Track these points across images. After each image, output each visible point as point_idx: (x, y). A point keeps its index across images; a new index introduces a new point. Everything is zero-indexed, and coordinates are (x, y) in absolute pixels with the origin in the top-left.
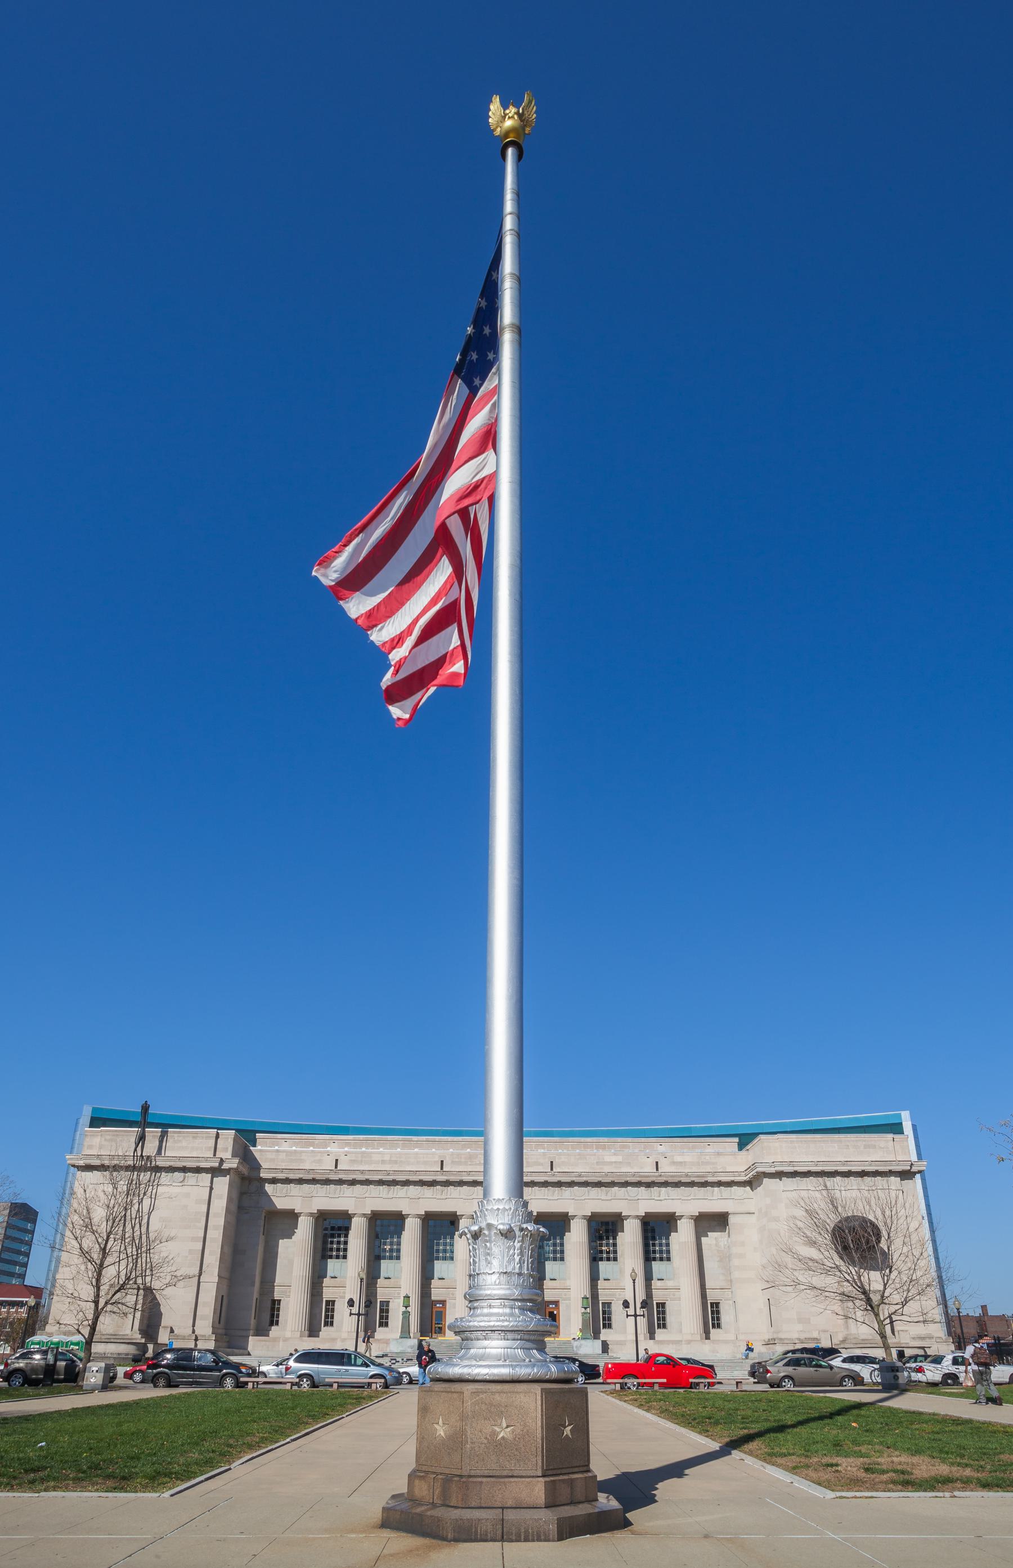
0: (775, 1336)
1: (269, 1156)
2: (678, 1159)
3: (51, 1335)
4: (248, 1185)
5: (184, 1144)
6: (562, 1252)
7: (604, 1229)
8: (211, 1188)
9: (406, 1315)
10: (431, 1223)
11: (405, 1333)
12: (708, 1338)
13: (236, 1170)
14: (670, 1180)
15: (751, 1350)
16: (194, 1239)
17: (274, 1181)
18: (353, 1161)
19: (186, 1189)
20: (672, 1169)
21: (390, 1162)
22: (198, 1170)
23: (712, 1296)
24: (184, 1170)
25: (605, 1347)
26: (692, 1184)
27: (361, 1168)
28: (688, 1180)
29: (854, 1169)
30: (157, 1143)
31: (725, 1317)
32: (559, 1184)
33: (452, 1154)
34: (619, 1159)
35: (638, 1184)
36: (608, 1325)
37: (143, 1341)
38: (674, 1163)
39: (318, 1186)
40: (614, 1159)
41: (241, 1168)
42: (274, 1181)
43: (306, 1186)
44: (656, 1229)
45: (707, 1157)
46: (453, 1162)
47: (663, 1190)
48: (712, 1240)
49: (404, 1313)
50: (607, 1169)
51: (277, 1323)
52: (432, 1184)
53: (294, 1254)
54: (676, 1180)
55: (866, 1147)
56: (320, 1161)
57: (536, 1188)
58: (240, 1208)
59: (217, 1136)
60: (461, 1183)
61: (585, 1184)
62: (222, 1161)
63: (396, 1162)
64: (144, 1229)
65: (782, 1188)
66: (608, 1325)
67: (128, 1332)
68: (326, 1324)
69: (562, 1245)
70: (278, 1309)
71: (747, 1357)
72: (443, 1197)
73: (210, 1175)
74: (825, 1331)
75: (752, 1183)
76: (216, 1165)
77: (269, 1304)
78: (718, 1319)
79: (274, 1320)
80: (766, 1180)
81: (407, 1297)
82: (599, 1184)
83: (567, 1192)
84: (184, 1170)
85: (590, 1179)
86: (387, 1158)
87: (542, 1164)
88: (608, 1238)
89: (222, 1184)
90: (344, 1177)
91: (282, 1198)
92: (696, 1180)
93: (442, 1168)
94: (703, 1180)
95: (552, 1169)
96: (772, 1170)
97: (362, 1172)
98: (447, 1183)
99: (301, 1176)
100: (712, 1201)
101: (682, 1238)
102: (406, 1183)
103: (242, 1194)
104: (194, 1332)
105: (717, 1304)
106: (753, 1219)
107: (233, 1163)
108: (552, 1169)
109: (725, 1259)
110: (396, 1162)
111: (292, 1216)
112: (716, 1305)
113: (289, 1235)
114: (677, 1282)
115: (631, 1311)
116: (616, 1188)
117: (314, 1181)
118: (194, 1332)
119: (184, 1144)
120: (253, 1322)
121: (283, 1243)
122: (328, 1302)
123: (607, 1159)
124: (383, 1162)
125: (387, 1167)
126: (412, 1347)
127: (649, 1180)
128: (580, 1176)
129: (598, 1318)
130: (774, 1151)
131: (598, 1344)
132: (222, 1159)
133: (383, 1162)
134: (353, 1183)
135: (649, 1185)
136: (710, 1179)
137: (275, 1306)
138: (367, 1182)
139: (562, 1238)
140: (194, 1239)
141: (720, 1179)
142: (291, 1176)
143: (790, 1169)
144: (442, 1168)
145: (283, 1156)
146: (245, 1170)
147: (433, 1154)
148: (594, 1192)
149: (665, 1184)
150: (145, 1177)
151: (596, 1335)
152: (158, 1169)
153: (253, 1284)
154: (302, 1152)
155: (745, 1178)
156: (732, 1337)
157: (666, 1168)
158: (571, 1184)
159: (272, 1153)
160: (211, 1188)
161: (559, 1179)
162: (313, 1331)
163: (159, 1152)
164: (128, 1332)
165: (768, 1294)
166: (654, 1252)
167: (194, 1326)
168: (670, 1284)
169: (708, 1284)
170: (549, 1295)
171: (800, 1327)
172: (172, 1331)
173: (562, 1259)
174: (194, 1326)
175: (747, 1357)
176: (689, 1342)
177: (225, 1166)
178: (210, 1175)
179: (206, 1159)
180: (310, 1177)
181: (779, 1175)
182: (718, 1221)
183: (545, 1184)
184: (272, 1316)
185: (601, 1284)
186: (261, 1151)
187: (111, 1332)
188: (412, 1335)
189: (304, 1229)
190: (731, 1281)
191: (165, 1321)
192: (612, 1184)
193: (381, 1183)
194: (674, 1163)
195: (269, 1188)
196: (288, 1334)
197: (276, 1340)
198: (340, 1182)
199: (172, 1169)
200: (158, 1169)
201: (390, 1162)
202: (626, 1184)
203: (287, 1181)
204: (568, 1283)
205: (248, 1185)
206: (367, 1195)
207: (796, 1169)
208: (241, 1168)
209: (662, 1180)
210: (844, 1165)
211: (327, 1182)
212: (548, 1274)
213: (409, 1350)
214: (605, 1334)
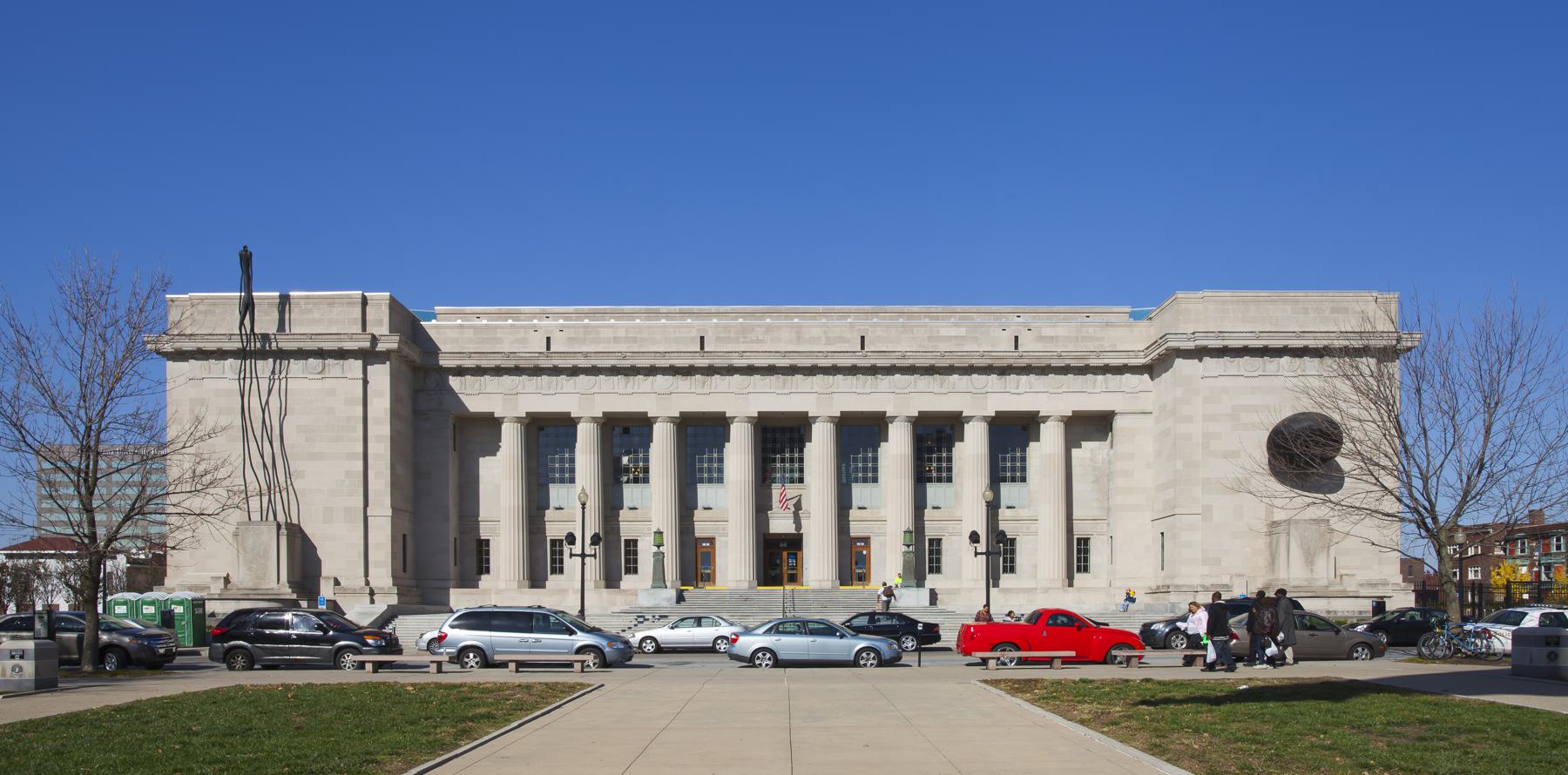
0: (1168, 582)
1: (450, 334)
2: (1048, 331)
3: (171, 591)
4: (421, 376)
5: (316, 315)
6: (875, 470)
7: (935, 438)
8: (365, 382)
9: (659, 558)
10: (690, 430)
11: (659, 580)
12: (1071, 585)
13: (398, 351)
14: (1035, 363)
15: (1132, 600)
16: (350, 456)
17: (460, 371)
18: (571, 340)
19: (328, 383)
20: (1039, 347)
21: (628, 340)
22: (342, 354)
23: (1079, 530)
24: (321, 354)
25: (933, 597)
26: (1065, 370)
27: (584, 349)
28: (1061, 363)
29: (1311, 343)
30: (276, 315)
31: (1096, 557)
32: (873, 370)
33: (717, 326)
34: (962, 332)
35: (988, 370)
36: (936, 569)
37: (294, 596)
38: (1041, 338)
39: (525, 377)
40: (953, 332)
41: (406, 350)
42: (460, 371)
43: (507, 379)
44: (1012, 433)
45: (1091, 330)
46: (718, 339)
47: (1024, 378)
48: (1088, 452)
49: (656, 554)
50: (943, 347)
51: (488, 571)
52: (689, 371)
53: (500, 477)
54: (1043, 363)
55: (1333, 311)
56: (524, 341)
57: (840, 377)
58: (417, 412)
59: (365, 302)
60: (730, 370)
61: (911, 370)
62: (374, 340)
63: (634, 340)
64: (277, 444)
65: (1201, 373)
66: (936, 569)
67: (273, 584)
68: (554, 571)
69: (875, 460)
70: (488, 553)
71: (1126, 610)
72: (706, 391)
73: (359, 363)
74: (1240, 575)
75: (1153, 369)
76: (368, 344)
77: (474, 546)
78: (1086, 560)
79: (483, 567)
80: (1179, 362)
81: (659, 533)
82: (930, 370)
83: (885, 382)
84: (321, 354)
85: (920, 362)
86: (621, 333)
87: (848, 341)
88: (940, 450)
89: (381, 375)
90: (562, 363)
91: (477, 396)
92: (1074, 363)
93: (702, 347)
94: (1081, 363)
95: (863, 347)
96: (1191, 345)
97: (586, 355)
98: (710, 371)
99: (498, 363)
100: (1091, 395)
101: (1045, 449)
102: (651, 371)
103: (416, 392)
104: (367, 583)
105: (1086, 541)
106: (1148, 422)
107: (389, 343)
108: (863, 347)
109: (1104, 478)
110: (634, 340)
111: (491, 423)
112: (1084, 542)
113: (493, 449)
114: (1034, 511)
115: (982, 547)
116: (956, 376)
117: (517, 371)
118: (367, 583)
119: (316, 315)
120: (453, 570)
121: (486, 464)
122: (553, 542)
123: (944, 332)
124: (616, 340)
125: (623, 347)
126: (668, 600)
127: (1004, 363)
128: (904, 357)
129: (924, 557)
130: (1200, 313)
131: (924, 595)
132: (374, 336)
133: (616, 340)
134: (574, 371)
135: (1004, 371)
136: (1094, 362)
137: (483, 548)
138: (594, 371)
139: (875, 451)
140: (350, 456)
141: (1107, 361)
142: (485, 363)
143: (1218, 344)
144: (702, 347)
145: (469, 334)
146: (414, 354)
147: (690, 327)
148: (924, 382)
149: (1027, 370)
150: (264, 367)
151: (920, 583)
152: (282, 355)
153: (446, 518)
154: (497, 327)
155: (1143, 361)
156: (1103, 583)
157: (1027, 345)
158: (891, 370)
159: (454, 331)
160: (365, 382)
161: (873, 362)
162: (536, 579)
163: (281, 327)
164: (273, 584)
165: (1162, 526)
166: (1004, 469)
167: (366, 575)
168: (1022, 513)
169: (1077, 513)
170: (856, 530)
171: (1206, 570)
172: (337, 583)
173: (875, 480)
174: (366, 575)
175: (1126, 610)
176: (1046, 590)
177: (381, 347)
178: (359, 363)
179: (351, 337)
180: (510, 364)
181: (1199, 353)
182: (1090, 426)
183: (853, 370)
184: (480, 561)
185: (928, 513)
186: (436, 327)
187: (250, 585)
188: (669, 584)
189: (511, 437)
190: (1109, 509)
191: (327, 570)
192: (950, 370)
193: (614, 371)
194: (1041, 338)
195: (454, 382)
196: (502, 585)
197: (486, 592)
198: (556, 371)
199: (302, 354)
200: (282, 355)
201: (628, 340)
202: (969, 370)
203: (479, 371)
204: (883, 513)
205: (421, 376)
206: (595, 390)
207: (1226, 343)
208: (406, 350)
209: (1023, 363)
210: (1298, 338)
211: (536, 371)
212: (856, 502)
213: (665, 604)
214: (932, 581)
